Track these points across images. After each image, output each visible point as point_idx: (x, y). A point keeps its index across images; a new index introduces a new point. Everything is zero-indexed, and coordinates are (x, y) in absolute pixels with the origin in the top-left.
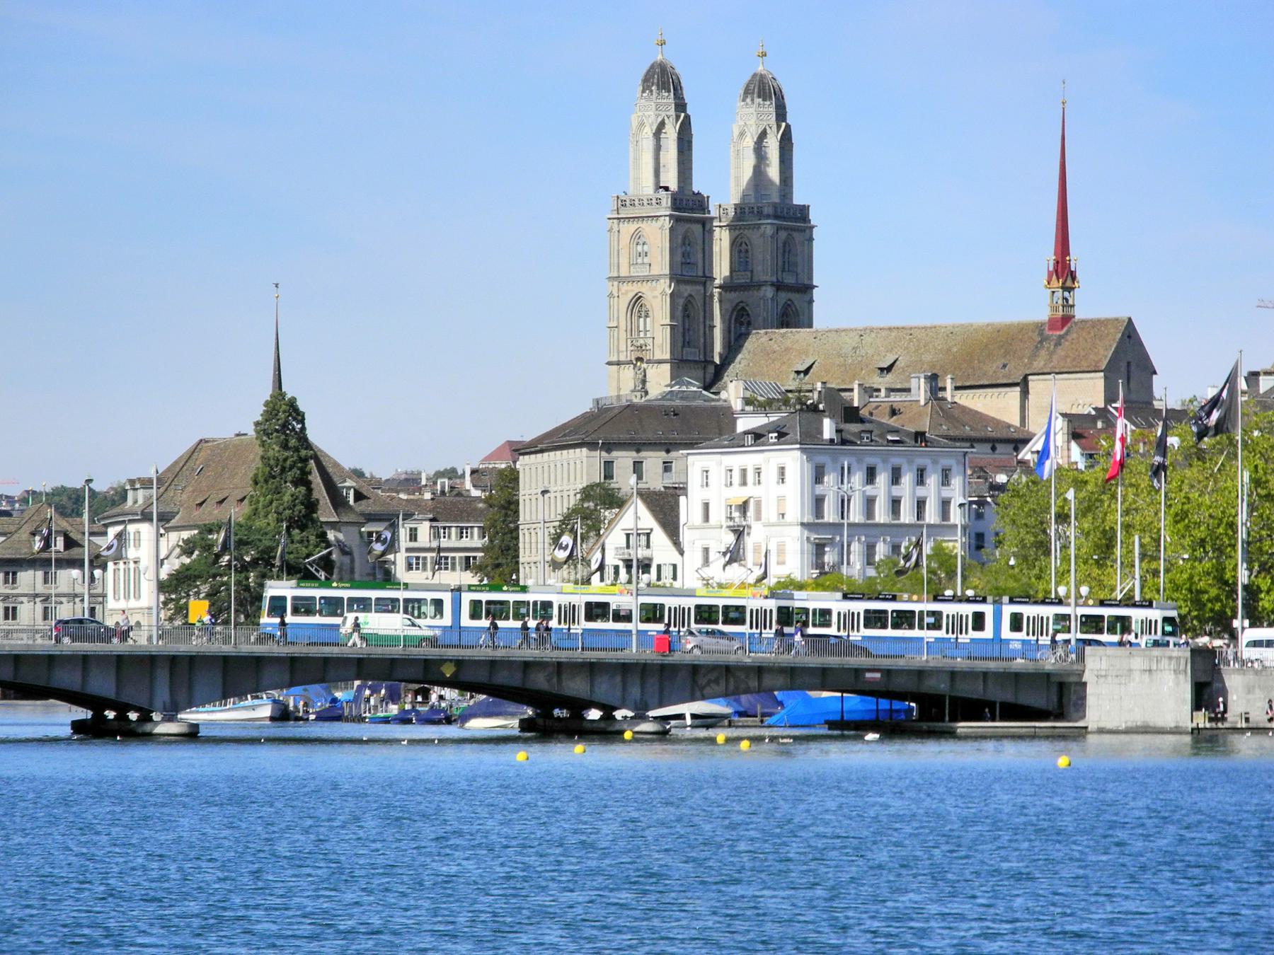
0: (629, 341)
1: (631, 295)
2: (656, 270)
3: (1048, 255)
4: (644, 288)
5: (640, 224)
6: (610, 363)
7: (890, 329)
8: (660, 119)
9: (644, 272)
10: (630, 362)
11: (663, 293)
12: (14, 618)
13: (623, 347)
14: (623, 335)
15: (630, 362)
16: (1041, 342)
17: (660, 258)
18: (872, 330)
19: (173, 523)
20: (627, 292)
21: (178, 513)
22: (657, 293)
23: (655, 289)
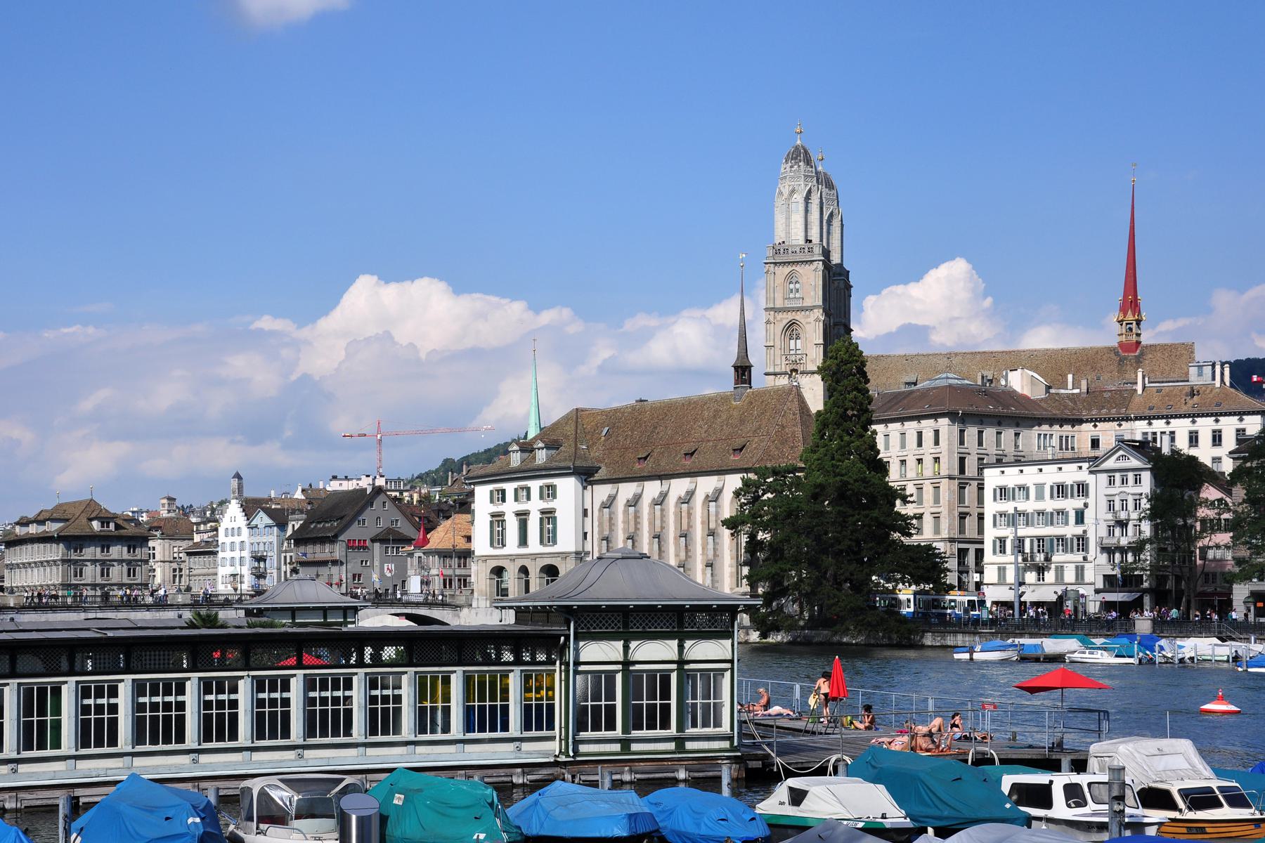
1: (788, 321)
2: (808, 303)
3: (1117, 293)
4: (799, 316)
5: (794, 267)
6: (766, 374)
7: (972, 353)
8: (808, 188)
10: (785, 373)
11: (817, 320)
12: (81, 576)
14: (778, 352)
15: (785, 373)
16: (1120, 360)
17: (812, 293)
18: (956, 354)
19: (597, 477)
20: (781, 320)
21: (600, 468)
22: (812, 319)
23: (808, 317)
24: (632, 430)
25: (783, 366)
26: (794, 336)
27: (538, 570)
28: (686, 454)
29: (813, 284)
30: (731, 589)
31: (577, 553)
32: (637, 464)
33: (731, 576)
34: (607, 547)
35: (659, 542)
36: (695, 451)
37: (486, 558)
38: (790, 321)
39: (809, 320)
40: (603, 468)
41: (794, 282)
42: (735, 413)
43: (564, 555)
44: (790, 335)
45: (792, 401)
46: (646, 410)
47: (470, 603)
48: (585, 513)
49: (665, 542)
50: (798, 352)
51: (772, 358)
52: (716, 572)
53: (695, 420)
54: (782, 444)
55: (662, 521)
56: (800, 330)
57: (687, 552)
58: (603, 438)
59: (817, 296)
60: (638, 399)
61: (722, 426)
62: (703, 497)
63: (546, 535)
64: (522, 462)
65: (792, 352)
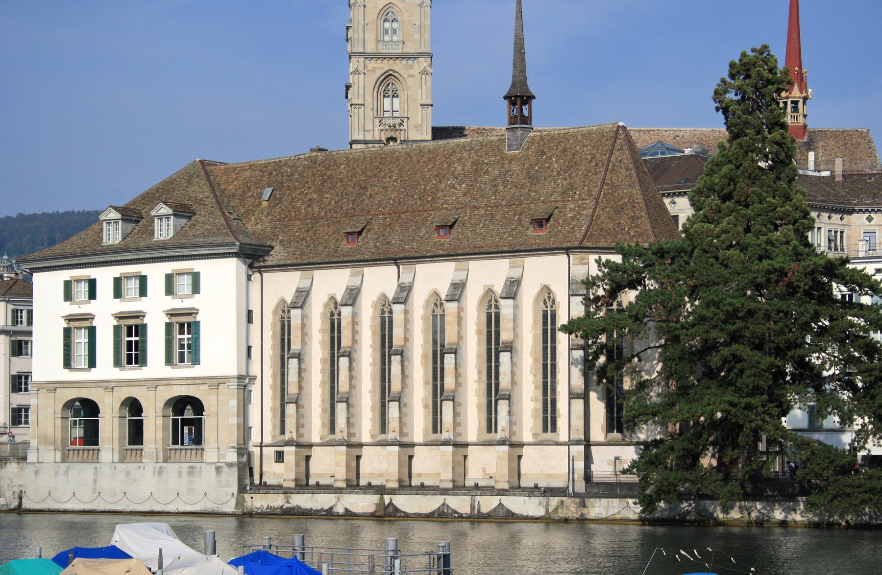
0: (377, 120)
1: (379, 73)
2: (410, 49)
4: (398, 66)
9: (398, 50)
13: (369, 126)
14: (369, 114)
19: (270, 260)
21: (273, 248)
22: (416, 71)
23: (411, 67)
24: (320, 192)
25: (376, 133)
26: (390, 93)
27: (161, 405)
28: (439, 227)
29: (418, 23)
30: (535, 435)
31: (240, 378)
32: (344, 242)
33: (534, 416)
34: (300, 368)
35: (402, 361)
36: (455, 223)
37: (53, 387)
38: (386, 72)
39: (412, 72)
40: (278, 248)
41: (391, 19)
42: (515, 167)
43: (216, 382)
44: (385, 90)
45: (621, 149)
46: (338, 161)
47: (21, 454)
48: (250, 320)
49: (409, 362)
50: (395, 114)
51: (362, 121)
52: (514, 409)
53: (440, 177)
54: (617, 212)
55: (406, 330)
56: (398, 85)
57: (457, 377)
58: (265, 204)
59: (423, 40)
60: (314, 147)
61: (495, 186)
62: (480, 292)
63: (176, 351)
64: (124, 239)
65: (386, 114)
